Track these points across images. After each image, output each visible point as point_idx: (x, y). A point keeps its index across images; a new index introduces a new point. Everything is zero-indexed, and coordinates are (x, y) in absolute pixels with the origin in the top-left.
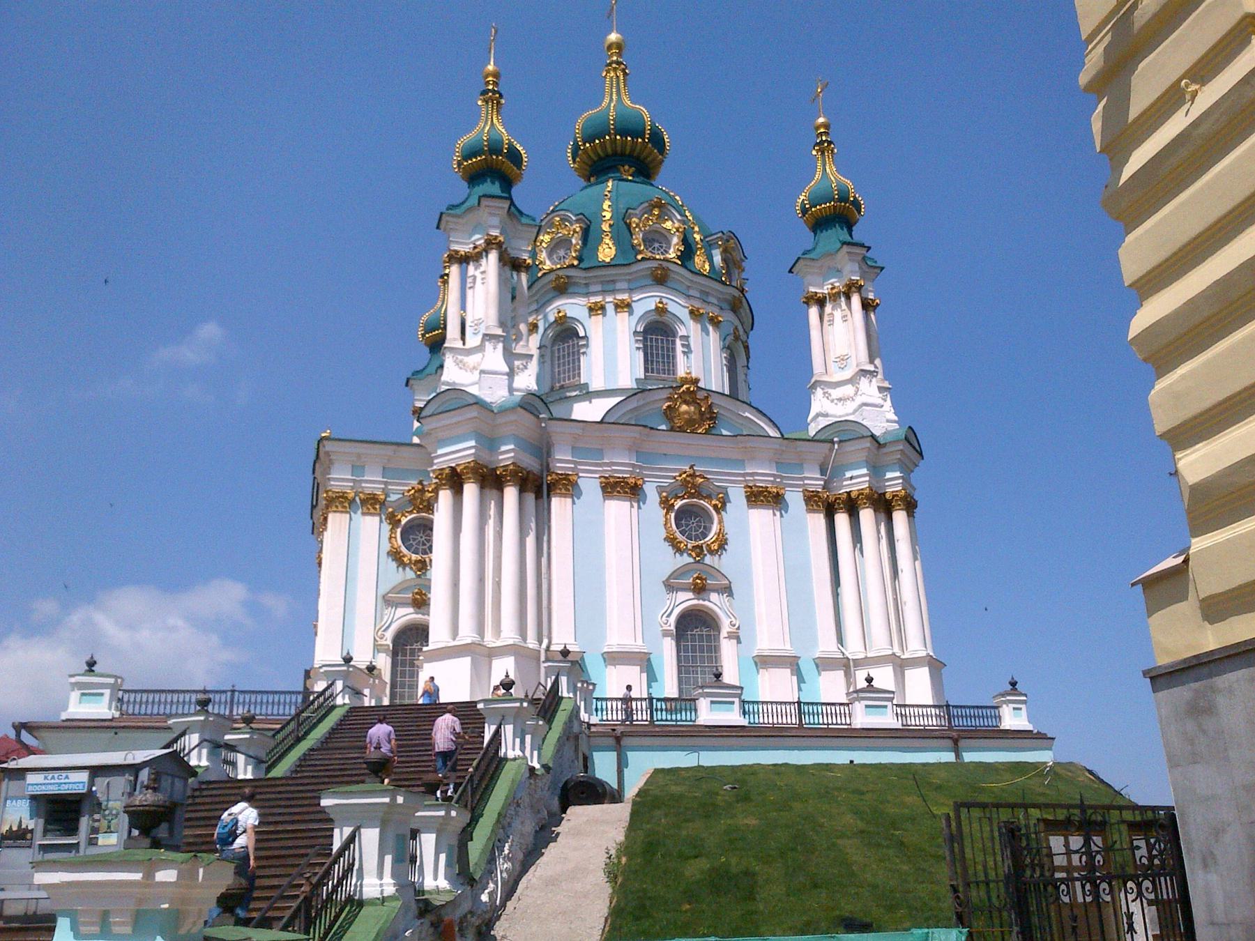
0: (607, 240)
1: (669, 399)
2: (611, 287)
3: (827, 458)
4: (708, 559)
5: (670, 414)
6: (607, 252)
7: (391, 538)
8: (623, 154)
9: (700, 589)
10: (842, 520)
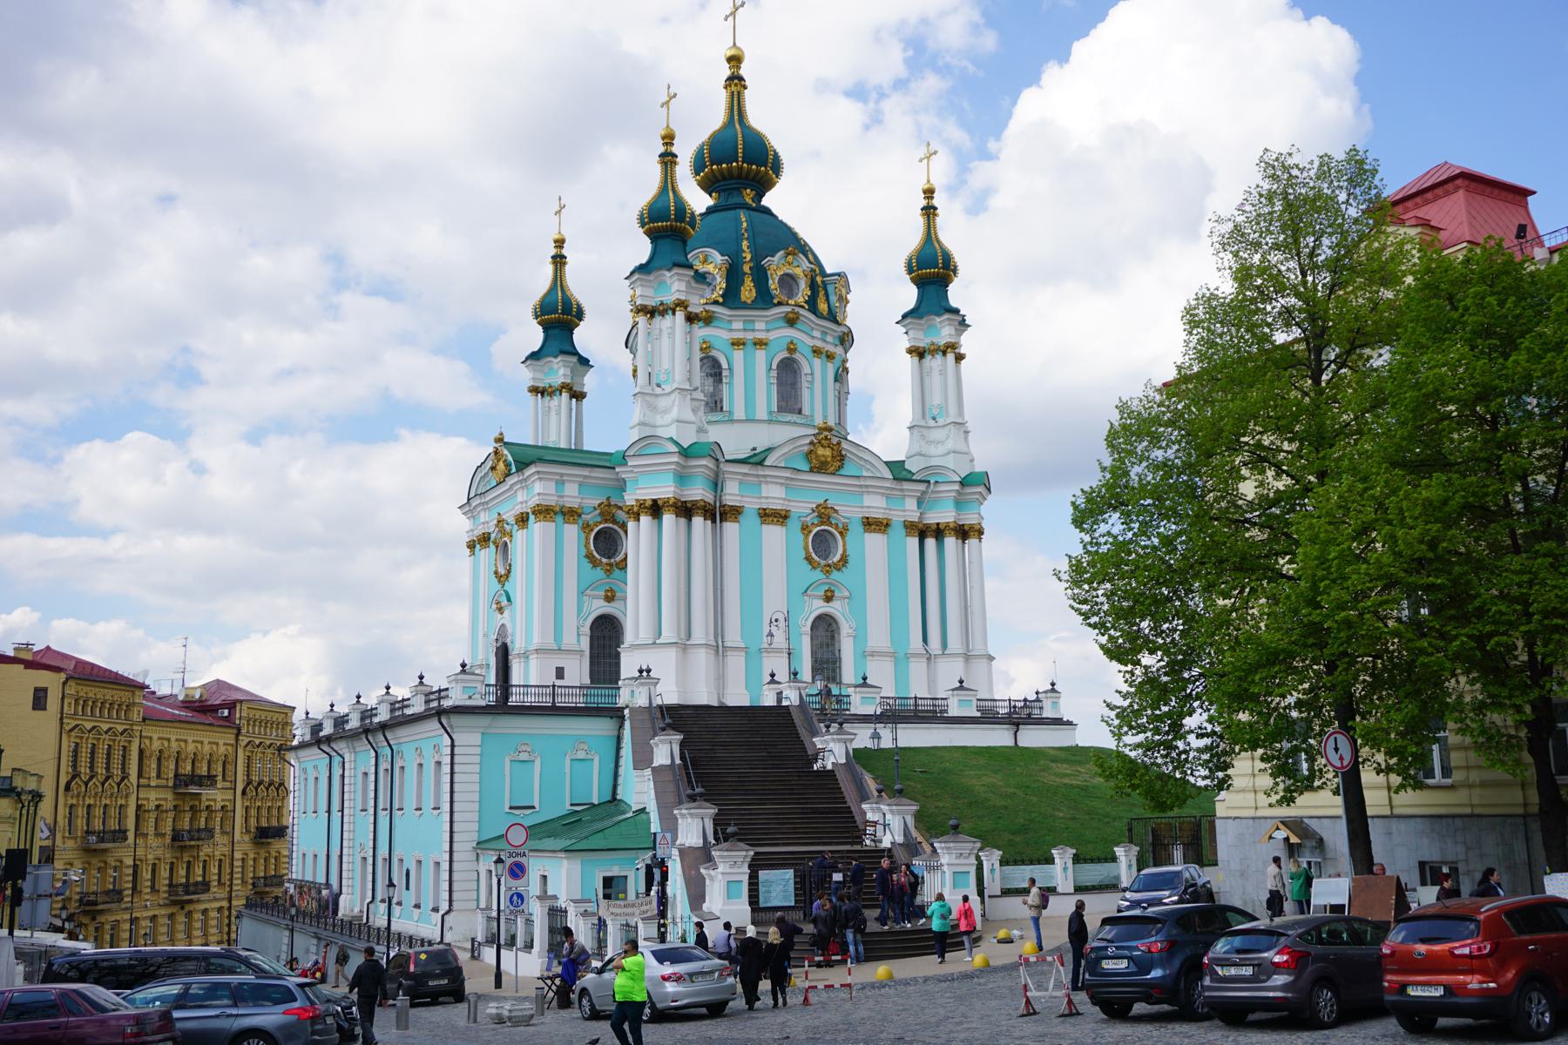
0: (749, 283)
1: (811, 443)
2: (749, 326)
3: (924, 493)
4: (835, 575)
5: (809, 455)
6: (748, 291)
7: (587, 545)
8: (747, 178)
9: (828, 598)
10: (930, 543)
